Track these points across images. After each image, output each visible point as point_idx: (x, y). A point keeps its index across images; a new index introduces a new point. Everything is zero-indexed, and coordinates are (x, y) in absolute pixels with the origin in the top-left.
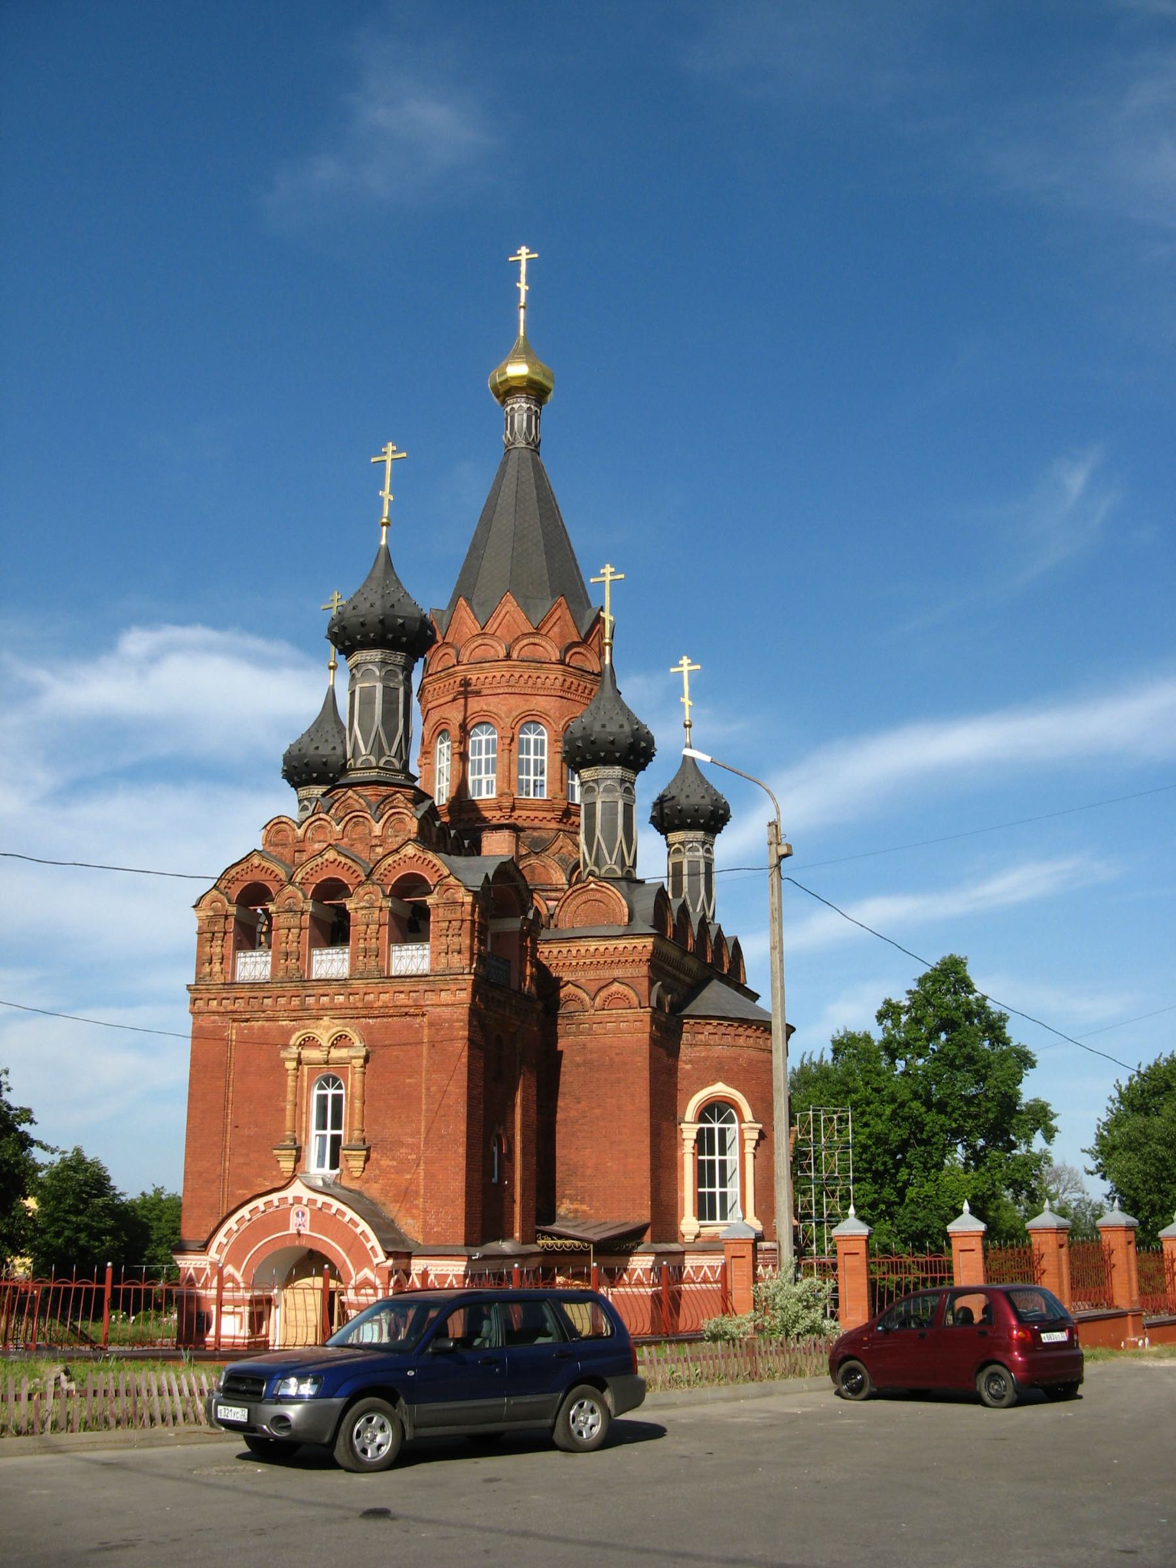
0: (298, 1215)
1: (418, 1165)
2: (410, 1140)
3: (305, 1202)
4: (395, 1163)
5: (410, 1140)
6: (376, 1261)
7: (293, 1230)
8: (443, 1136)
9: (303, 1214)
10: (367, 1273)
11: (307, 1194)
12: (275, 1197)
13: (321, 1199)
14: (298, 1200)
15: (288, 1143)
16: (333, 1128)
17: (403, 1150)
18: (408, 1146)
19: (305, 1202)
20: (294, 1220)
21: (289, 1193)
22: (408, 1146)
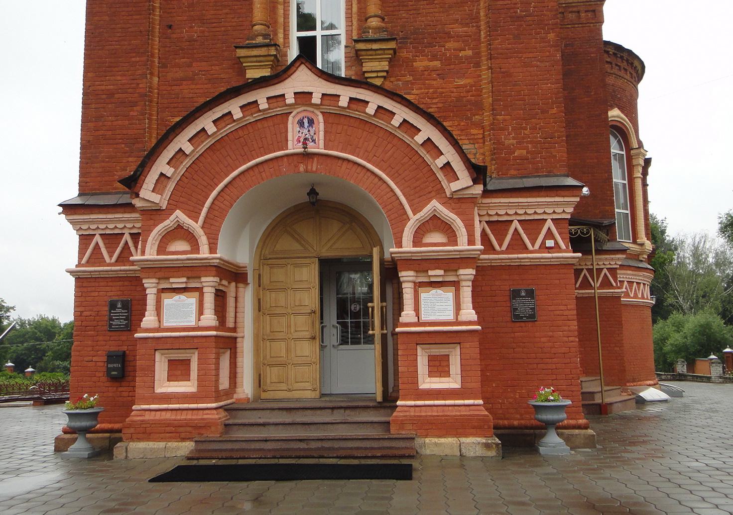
0: (301, 124)
1: (478, 65)
2: (461, 30)
3: (316, 99)
4: (437, 64)
5: (461, 30)
6: (455, 186)
7: (294, 147)
8: (520, 18)
9: (311, 122)
10: (435, 205)
11: (318, 88)
12: (261, 97)
13: (345, 94)
14: (303, 97)
15: (260, 40)
16: (314, 38)
17: (451, 45)
18: (458, 37)
19: (316, 99)
20: (293, 132)
21: (288, 88)
22: (458, 37)
